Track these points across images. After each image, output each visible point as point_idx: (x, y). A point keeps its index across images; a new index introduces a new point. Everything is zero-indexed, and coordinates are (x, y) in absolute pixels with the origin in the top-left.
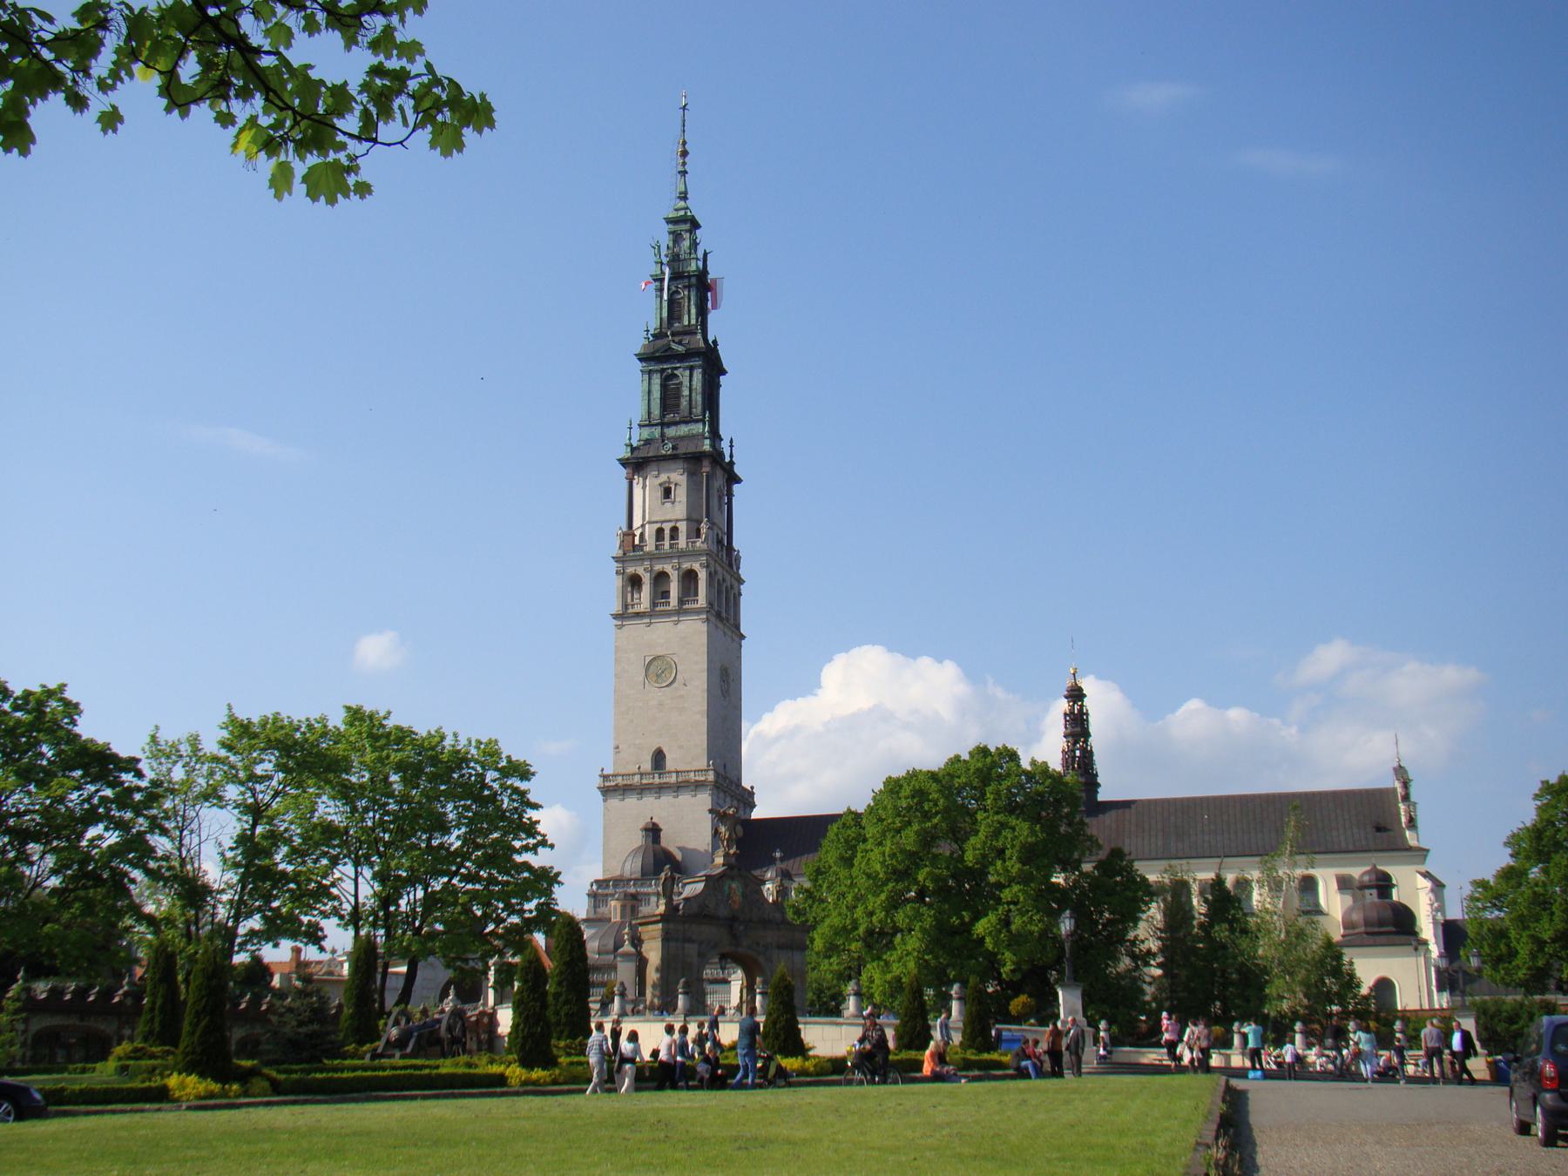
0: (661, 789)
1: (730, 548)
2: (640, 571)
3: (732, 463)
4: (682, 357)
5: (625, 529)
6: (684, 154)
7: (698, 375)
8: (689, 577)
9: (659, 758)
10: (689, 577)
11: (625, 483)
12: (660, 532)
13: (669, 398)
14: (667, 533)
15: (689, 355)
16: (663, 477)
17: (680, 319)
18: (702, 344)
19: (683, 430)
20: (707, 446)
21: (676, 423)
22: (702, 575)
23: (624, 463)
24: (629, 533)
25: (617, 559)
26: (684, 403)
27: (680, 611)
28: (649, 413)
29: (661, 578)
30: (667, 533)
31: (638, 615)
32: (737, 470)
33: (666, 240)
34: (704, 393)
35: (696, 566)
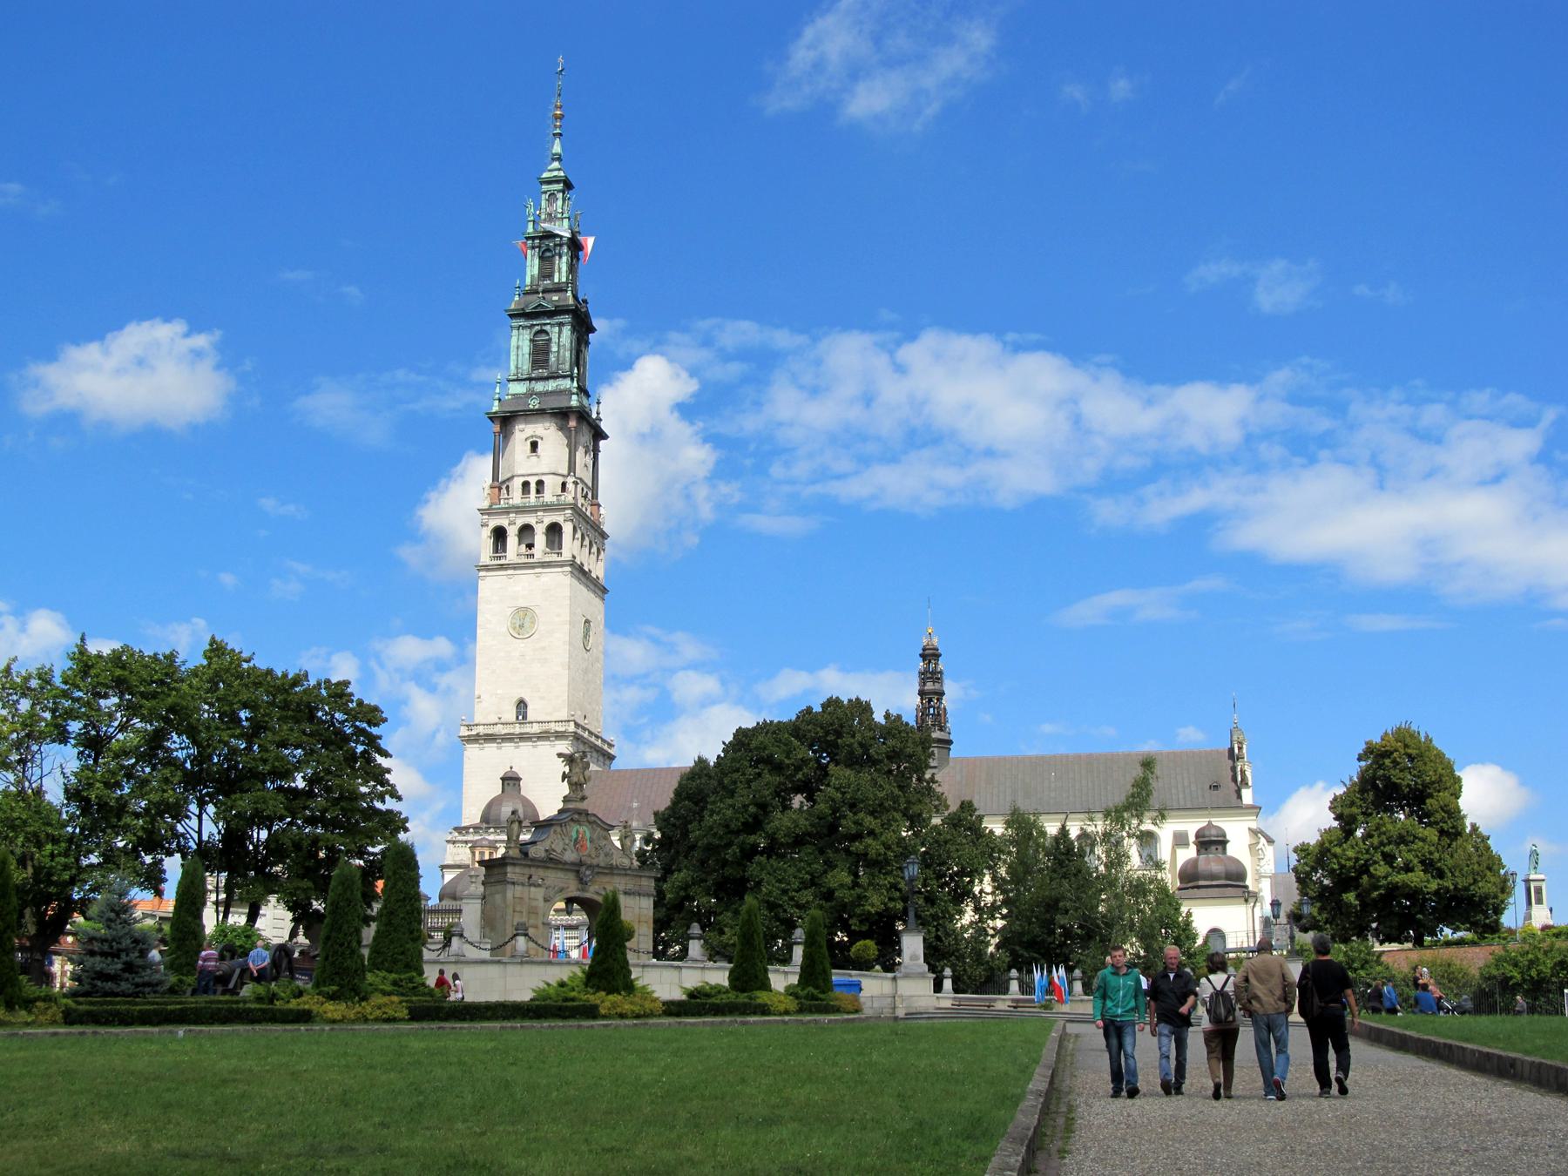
0: (524, 737)
4: (551, 314)
7: (567, 331)
8: (554, 530)
9: (522, 705)
10: (554, 530)
12: (526, 485)
13: (540, 354)
14: (533, 487)
15: (559, 311)
17: (550, 276)
18: (571, 301)
19: (551, 385)
20: (574, 401)
22: (567, 529)
26: (553, 358)
29: (526, 530)
30: (533, 487)
31: (502, 567)
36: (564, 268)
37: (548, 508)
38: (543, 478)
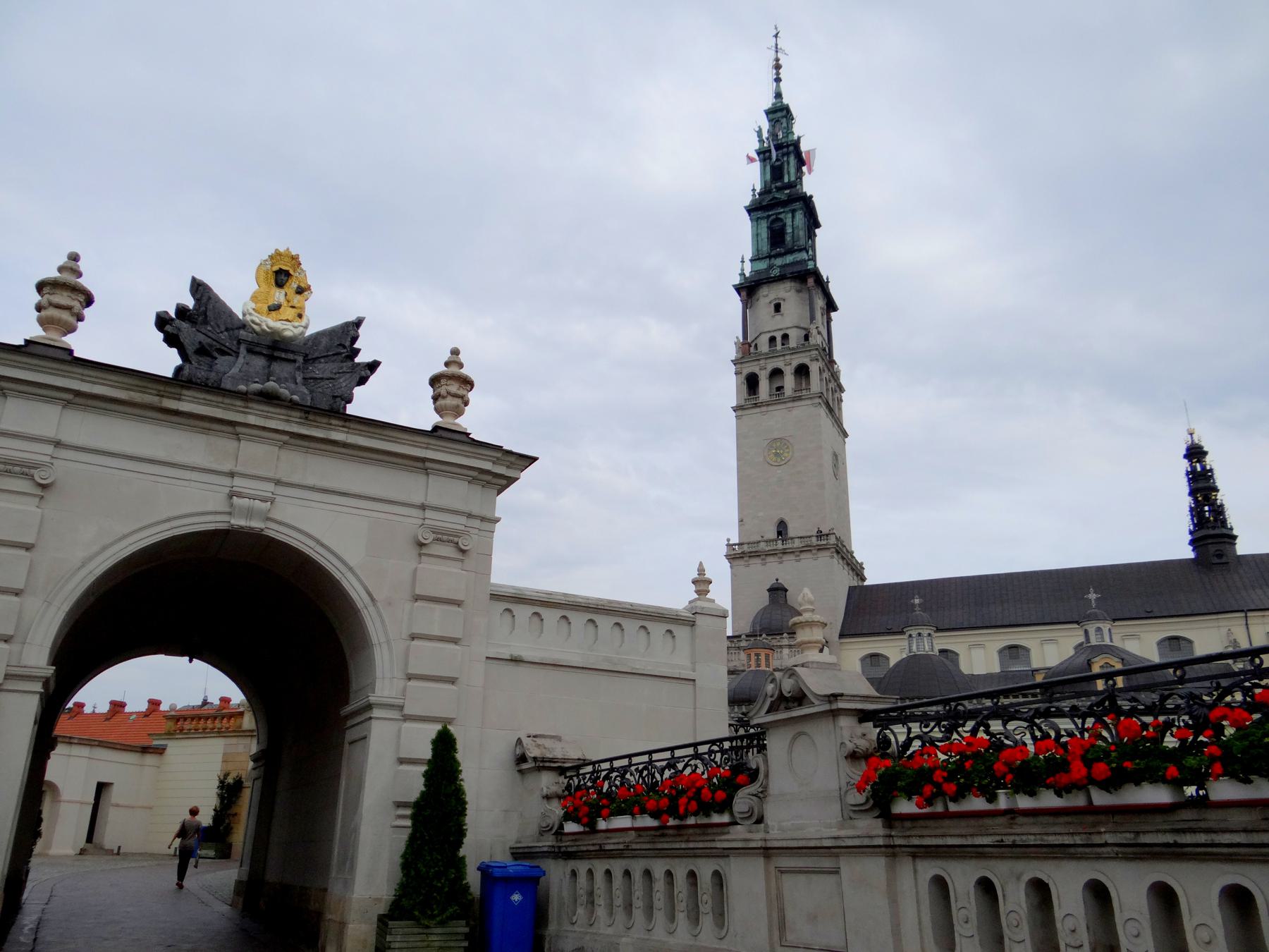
2: (756, 370)
4: (784, 204)
6: (778, 67)
7: (800, 218)
8: (802, 371)
10: (802, 371)
11: (740, 305)
12: (773, 339)
14: (779, 340)
16: (772, 296)
17: (781, 177)
19: (789, 259)
22: (814, 368)
23: (738, 289)
25: (735, 362)
26: (788, 238)
27: (795, 399)
29: (776, 373)
30: (779, 340)
31: (756, 405)
33: (766, 126)
35: (806, 361)
36: (793, 170)
37: (794, 351)
38: (788, 332)
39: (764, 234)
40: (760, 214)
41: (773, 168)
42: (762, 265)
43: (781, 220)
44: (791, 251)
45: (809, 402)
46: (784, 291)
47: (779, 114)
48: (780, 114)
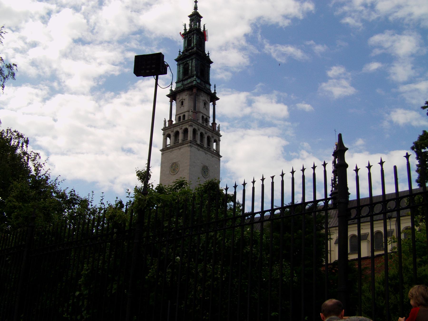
1: (214, 124)
2: (170, 132)
3: (215, 93)
5: (168, 119)
7: (194, 61)
10: (186, 131)
12: (180, 117)
14: (182, 117)
16: (181, 98)
19: (189, 81)
21: (187, 79)
23: (168, 96)
24: (170, 121)
25: (163, 130)
26: (190, 72)
27: (182, 144)
28: (179, 78)
29: (177, 134)
30: (182, 117)
31: (168, 149)
32: (217, 95)
34: (196, 68)
35: (187, 127)
36: (195, 41)
38: (185, 114)
39: (181, 71)
40: (180, 62)
41: (188, 41)
42: (180, 85)
43: (188, 64)
44: (190, 78)
45: (186, 145)
46: (185, 96)
47: (194, 17)
48: (196, 17)
